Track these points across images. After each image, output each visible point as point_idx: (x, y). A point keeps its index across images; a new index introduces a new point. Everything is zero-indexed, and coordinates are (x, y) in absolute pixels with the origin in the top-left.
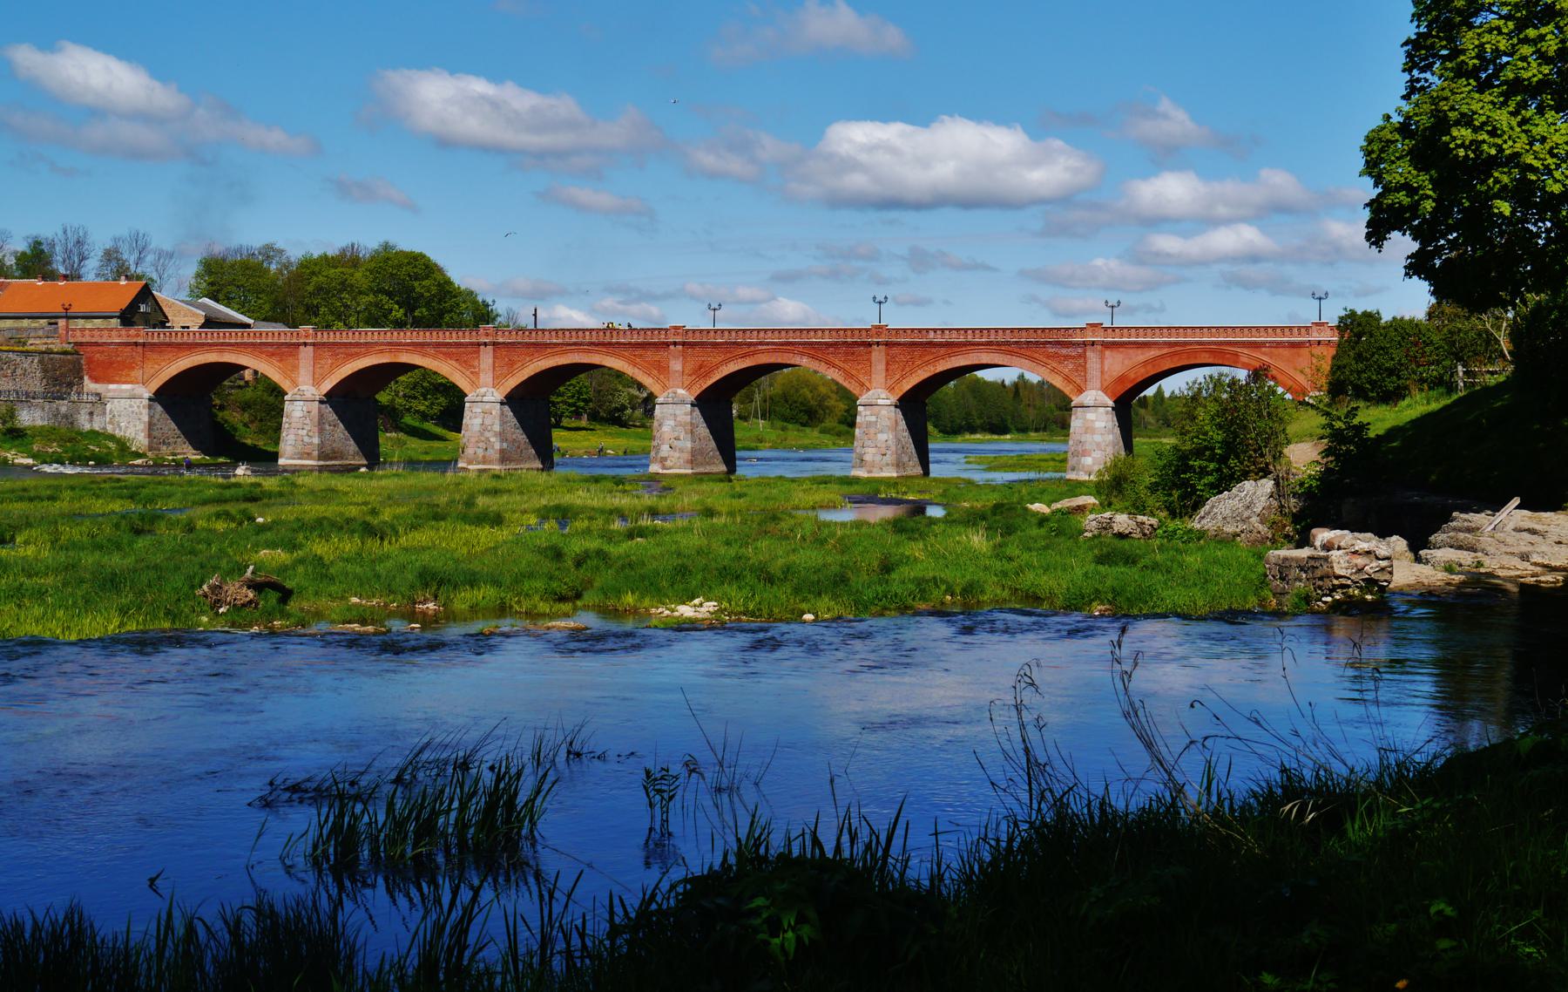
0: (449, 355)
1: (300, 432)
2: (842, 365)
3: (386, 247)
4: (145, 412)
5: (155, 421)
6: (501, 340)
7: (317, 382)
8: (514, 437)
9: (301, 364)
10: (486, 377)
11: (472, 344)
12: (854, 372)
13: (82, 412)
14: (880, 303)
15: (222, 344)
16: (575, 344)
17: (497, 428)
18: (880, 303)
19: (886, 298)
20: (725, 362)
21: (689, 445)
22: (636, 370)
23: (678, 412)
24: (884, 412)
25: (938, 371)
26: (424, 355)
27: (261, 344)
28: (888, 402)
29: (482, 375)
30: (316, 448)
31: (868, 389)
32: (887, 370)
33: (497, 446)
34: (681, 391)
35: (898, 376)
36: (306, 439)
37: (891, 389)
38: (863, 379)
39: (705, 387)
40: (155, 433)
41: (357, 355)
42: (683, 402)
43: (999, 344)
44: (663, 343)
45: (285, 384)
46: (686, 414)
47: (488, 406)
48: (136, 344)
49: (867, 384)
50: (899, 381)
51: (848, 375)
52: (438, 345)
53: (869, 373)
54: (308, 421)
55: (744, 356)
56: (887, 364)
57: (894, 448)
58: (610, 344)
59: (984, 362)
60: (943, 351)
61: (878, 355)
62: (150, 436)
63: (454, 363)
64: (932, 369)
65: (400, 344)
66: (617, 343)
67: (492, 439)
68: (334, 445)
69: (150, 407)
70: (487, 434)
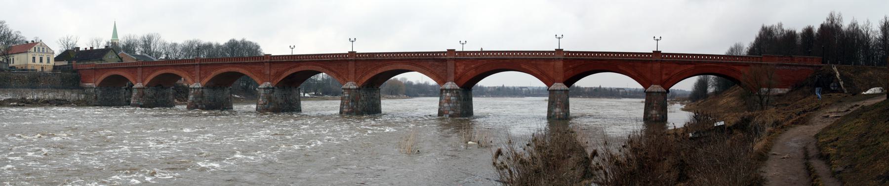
2: (335, 70)
3: (243, 40)
15: (116, 68)
19: (355, 39)
25: (378, 73)
31: (347, 82)
32: (355, 73)
34: (268, 83)
37: (357, 82)
41: (155, 71)
48: (92, 69)
49: (346, 79)
50: (361, 78)
55: (294, 67)
56: (356, 70)
59: (407, 69)
60: (380, 64)
61: (351, 65)
63: (186, 72)
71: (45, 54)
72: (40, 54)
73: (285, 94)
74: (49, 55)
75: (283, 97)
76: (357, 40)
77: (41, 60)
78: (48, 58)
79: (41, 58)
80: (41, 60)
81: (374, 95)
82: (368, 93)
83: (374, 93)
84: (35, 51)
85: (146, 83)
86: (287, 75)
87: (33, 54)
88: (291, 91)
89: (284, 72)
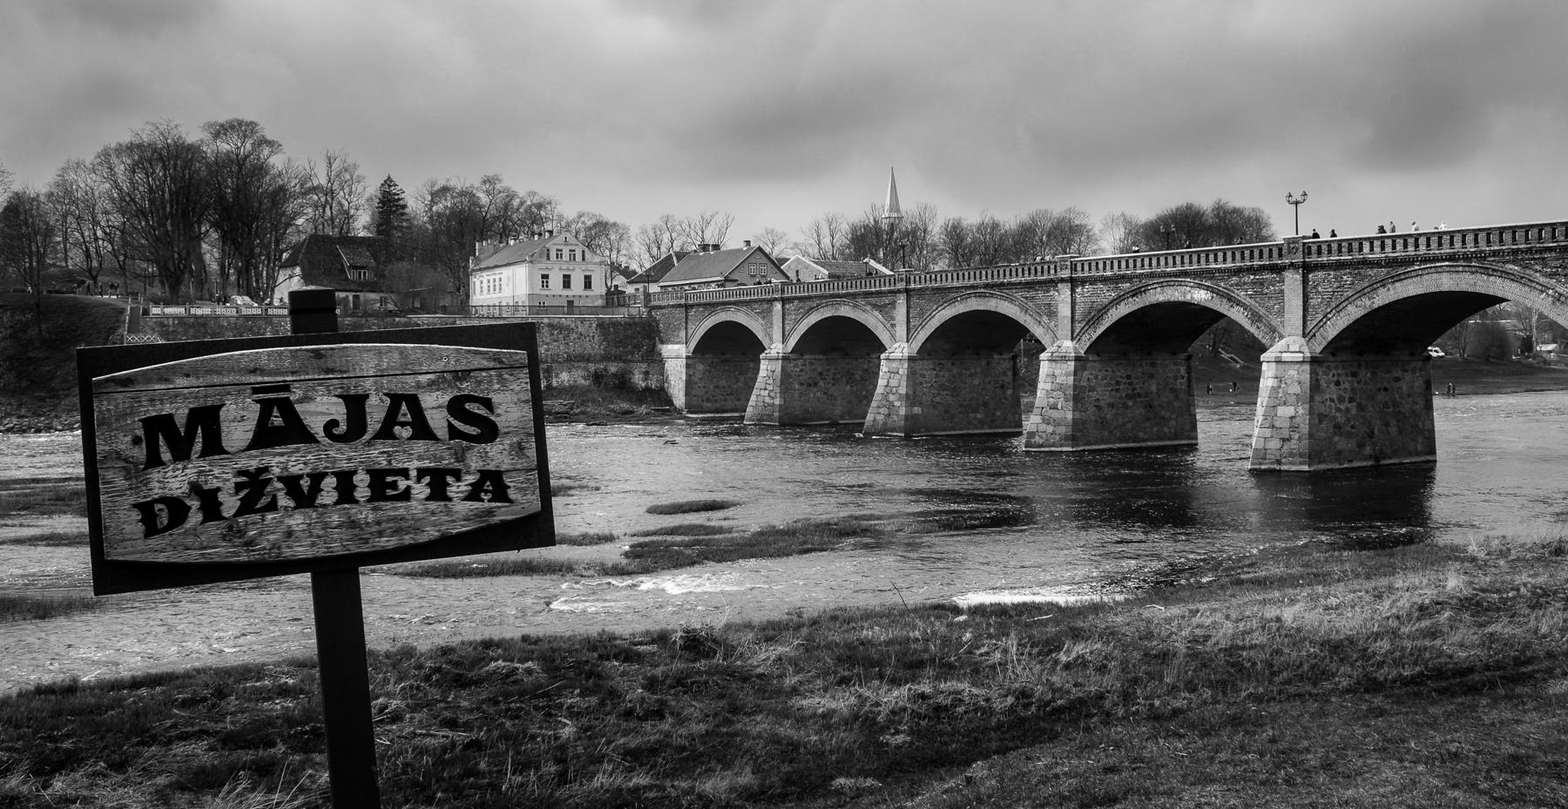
0: (875, 306)
1: (762, 393)
2: (1248, 301)
4: (684, 370)
5: (696, 379)
6: (912, 286)
7: (784, 339)
8: (938, 399)
9: (774, 322)
10: (901, 330)
11: (891, 292)
12: (1262, 312)
13: (636, 372)
14: (1297, 203)
16: (972, 287)
17: (903, 390)
18: (1297, 203)
20: (1116, 302)
21: (1069, 416)
22: (1028, 318)
23: (1057, 372)
24: (1292, 372)
25: (1376, 306)
26: (855, 306)
27: (751, 301)
28: (1299, 357)
29: (897, 328)
30: (777, 409)
31: (1281, 337)
33: (902, 412)
35: (1320, 317)
36: (767, 400)
38: (1275, 321)
39: (1094, 337)
40: (693, 393)
42: (1064, 359)
43: (1467, 258)
44: (1052, 281)
45: (765, 342)
46: (1067, 375)
47: (895, 365)
51: (1256, 318)
52: (867, 295)
53: (1281, 312)
54: (771, 381)
57: (1305, 429)
58: (1002, 284)
62: (687, 394)
64: (1368, 303)
65: (838, 296)
66: (1009, 283)
67: (897, 404)
68: (808, 405)
69: (688, 366)
70: (892, 398)
71: (577, 267)
72: (564, 267)
73: (1128, 377)
74: (590, 267)
75: (1118, 383)
76: (1309, 198)
77: (567, 282)
78: (565, 276)
79: (565, 276)
80: (567, 282)
81: (1397, 379)
82: (1365, 374)
83: (1399, 374)
84: (548, 258)
85: (792, 342)
86: (1115, 318)
87: (543, 266)
88: (1153, 365)
89: (1104, 309)
